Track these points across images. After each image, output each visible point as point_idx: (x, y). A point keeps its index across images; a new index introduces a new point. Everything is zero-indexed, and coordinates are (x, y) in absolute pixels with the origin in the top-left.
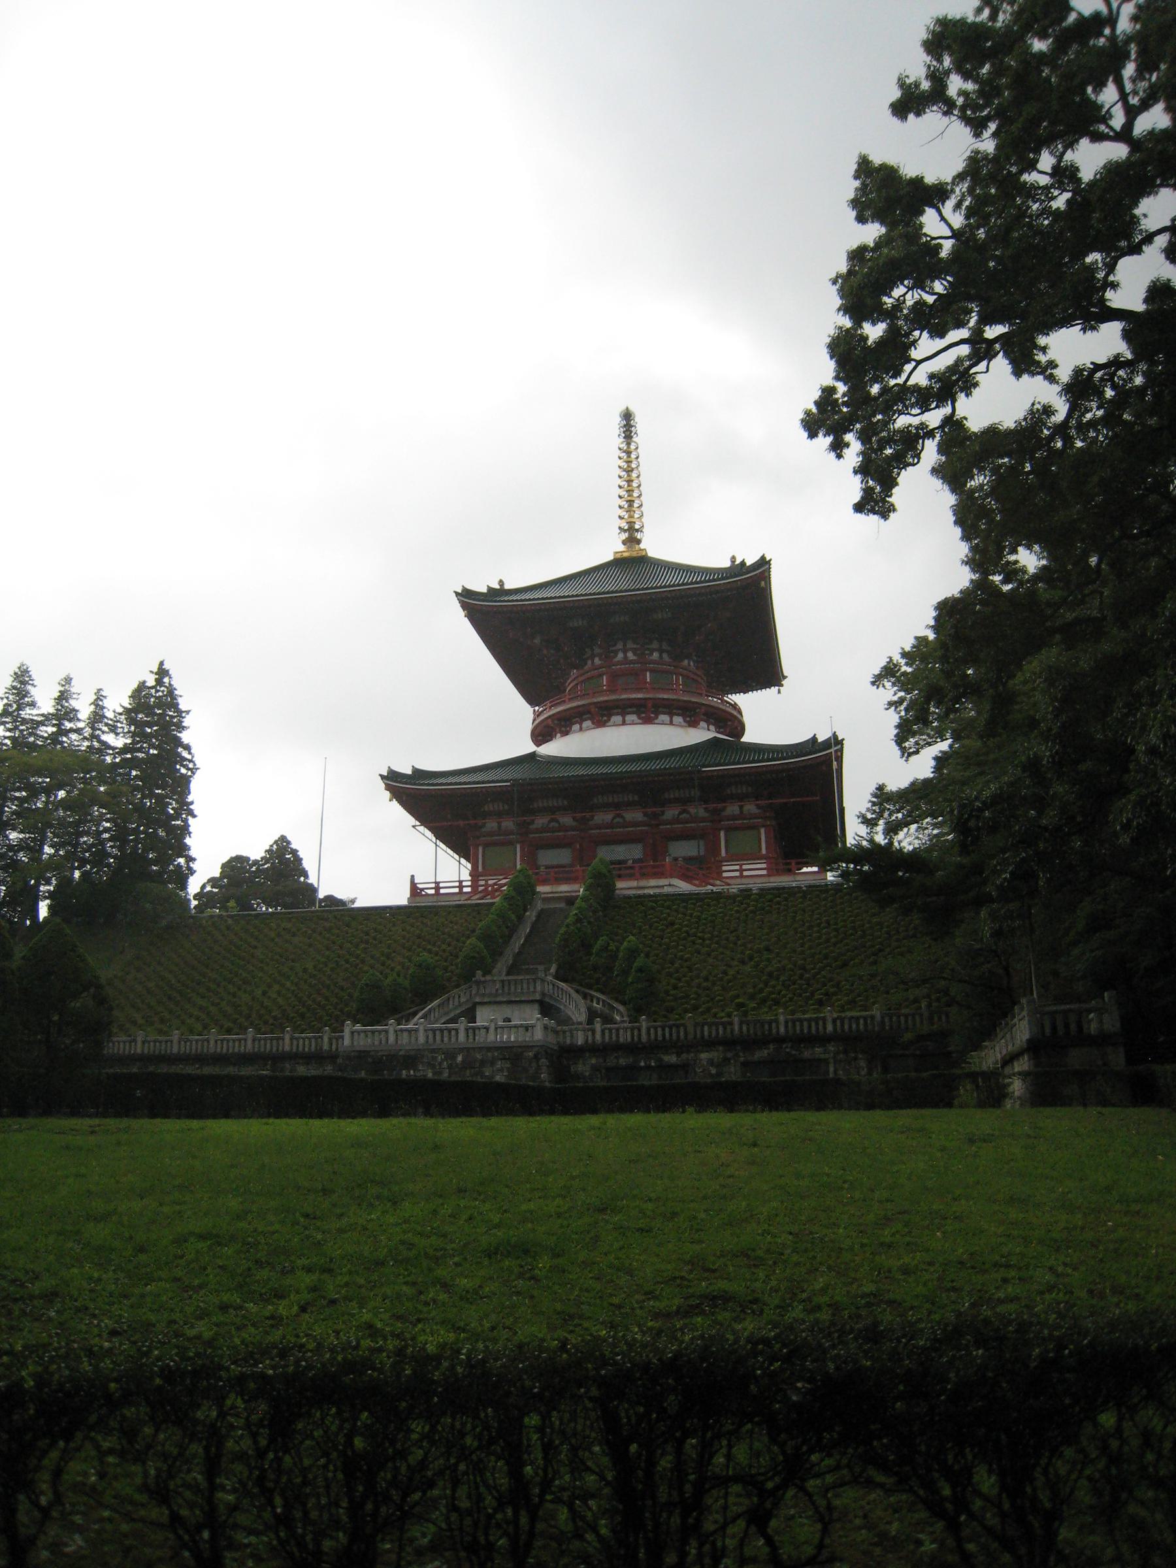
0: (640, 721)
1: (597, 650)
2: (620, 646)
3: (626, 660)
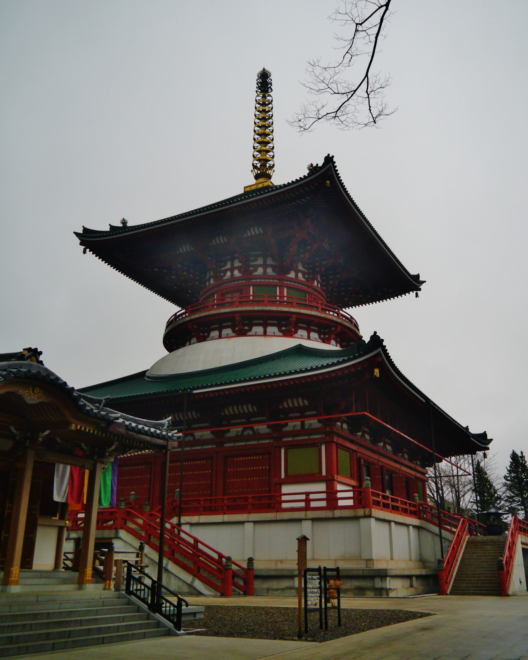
0: (281, 334)
1: (237, 264)
2: (260, 261)
3: (265, 275)
